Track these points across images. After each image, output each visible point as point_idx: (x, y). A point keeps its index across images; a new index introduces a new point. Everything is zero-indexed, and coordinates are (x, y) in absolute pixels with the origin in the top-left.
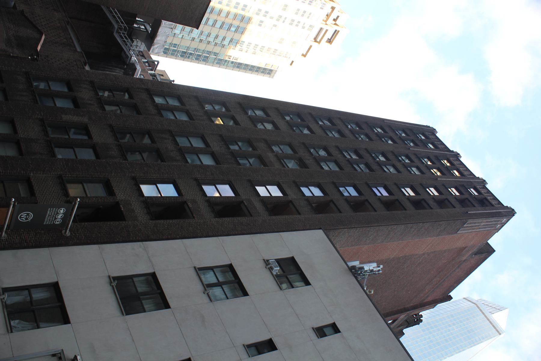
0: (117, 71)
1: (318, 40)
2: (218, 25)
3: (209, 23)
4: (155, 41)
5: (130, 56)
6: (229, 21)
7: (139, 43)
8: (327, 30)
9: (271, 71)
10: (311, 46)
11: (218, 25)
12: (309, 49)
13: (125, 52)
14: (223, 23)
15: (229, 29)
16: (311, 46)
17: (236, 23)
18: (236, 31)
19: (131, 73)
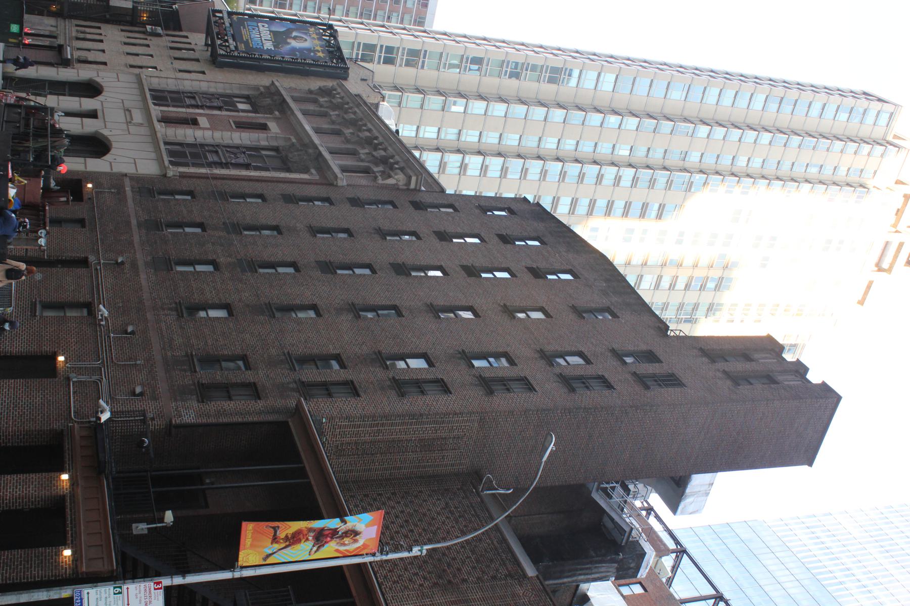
0: (603, 569)
1: (885, 265)
2: (681, 285)
3: (662, 284)
4: (688, 491)
5: (627, 529)
6: (700, 273)
7: (640, 486)
8: (901, 245)
9: (795, 346)
10: (871, 283)
11: (681, 285)
12: (869, 287)
13: (612, 520)
14: (691, 279)
15: (702, 288)
16: (871, 283)
17: (715, 274)
18: (717, 288)
19: (632, 565)
